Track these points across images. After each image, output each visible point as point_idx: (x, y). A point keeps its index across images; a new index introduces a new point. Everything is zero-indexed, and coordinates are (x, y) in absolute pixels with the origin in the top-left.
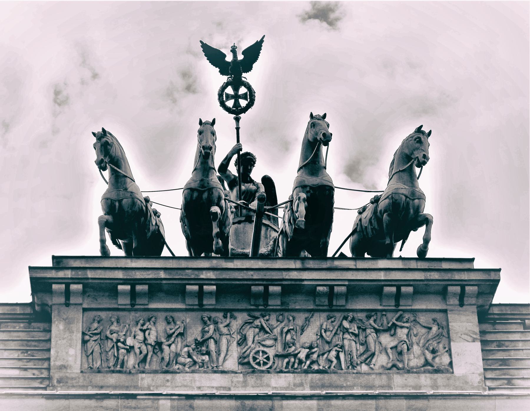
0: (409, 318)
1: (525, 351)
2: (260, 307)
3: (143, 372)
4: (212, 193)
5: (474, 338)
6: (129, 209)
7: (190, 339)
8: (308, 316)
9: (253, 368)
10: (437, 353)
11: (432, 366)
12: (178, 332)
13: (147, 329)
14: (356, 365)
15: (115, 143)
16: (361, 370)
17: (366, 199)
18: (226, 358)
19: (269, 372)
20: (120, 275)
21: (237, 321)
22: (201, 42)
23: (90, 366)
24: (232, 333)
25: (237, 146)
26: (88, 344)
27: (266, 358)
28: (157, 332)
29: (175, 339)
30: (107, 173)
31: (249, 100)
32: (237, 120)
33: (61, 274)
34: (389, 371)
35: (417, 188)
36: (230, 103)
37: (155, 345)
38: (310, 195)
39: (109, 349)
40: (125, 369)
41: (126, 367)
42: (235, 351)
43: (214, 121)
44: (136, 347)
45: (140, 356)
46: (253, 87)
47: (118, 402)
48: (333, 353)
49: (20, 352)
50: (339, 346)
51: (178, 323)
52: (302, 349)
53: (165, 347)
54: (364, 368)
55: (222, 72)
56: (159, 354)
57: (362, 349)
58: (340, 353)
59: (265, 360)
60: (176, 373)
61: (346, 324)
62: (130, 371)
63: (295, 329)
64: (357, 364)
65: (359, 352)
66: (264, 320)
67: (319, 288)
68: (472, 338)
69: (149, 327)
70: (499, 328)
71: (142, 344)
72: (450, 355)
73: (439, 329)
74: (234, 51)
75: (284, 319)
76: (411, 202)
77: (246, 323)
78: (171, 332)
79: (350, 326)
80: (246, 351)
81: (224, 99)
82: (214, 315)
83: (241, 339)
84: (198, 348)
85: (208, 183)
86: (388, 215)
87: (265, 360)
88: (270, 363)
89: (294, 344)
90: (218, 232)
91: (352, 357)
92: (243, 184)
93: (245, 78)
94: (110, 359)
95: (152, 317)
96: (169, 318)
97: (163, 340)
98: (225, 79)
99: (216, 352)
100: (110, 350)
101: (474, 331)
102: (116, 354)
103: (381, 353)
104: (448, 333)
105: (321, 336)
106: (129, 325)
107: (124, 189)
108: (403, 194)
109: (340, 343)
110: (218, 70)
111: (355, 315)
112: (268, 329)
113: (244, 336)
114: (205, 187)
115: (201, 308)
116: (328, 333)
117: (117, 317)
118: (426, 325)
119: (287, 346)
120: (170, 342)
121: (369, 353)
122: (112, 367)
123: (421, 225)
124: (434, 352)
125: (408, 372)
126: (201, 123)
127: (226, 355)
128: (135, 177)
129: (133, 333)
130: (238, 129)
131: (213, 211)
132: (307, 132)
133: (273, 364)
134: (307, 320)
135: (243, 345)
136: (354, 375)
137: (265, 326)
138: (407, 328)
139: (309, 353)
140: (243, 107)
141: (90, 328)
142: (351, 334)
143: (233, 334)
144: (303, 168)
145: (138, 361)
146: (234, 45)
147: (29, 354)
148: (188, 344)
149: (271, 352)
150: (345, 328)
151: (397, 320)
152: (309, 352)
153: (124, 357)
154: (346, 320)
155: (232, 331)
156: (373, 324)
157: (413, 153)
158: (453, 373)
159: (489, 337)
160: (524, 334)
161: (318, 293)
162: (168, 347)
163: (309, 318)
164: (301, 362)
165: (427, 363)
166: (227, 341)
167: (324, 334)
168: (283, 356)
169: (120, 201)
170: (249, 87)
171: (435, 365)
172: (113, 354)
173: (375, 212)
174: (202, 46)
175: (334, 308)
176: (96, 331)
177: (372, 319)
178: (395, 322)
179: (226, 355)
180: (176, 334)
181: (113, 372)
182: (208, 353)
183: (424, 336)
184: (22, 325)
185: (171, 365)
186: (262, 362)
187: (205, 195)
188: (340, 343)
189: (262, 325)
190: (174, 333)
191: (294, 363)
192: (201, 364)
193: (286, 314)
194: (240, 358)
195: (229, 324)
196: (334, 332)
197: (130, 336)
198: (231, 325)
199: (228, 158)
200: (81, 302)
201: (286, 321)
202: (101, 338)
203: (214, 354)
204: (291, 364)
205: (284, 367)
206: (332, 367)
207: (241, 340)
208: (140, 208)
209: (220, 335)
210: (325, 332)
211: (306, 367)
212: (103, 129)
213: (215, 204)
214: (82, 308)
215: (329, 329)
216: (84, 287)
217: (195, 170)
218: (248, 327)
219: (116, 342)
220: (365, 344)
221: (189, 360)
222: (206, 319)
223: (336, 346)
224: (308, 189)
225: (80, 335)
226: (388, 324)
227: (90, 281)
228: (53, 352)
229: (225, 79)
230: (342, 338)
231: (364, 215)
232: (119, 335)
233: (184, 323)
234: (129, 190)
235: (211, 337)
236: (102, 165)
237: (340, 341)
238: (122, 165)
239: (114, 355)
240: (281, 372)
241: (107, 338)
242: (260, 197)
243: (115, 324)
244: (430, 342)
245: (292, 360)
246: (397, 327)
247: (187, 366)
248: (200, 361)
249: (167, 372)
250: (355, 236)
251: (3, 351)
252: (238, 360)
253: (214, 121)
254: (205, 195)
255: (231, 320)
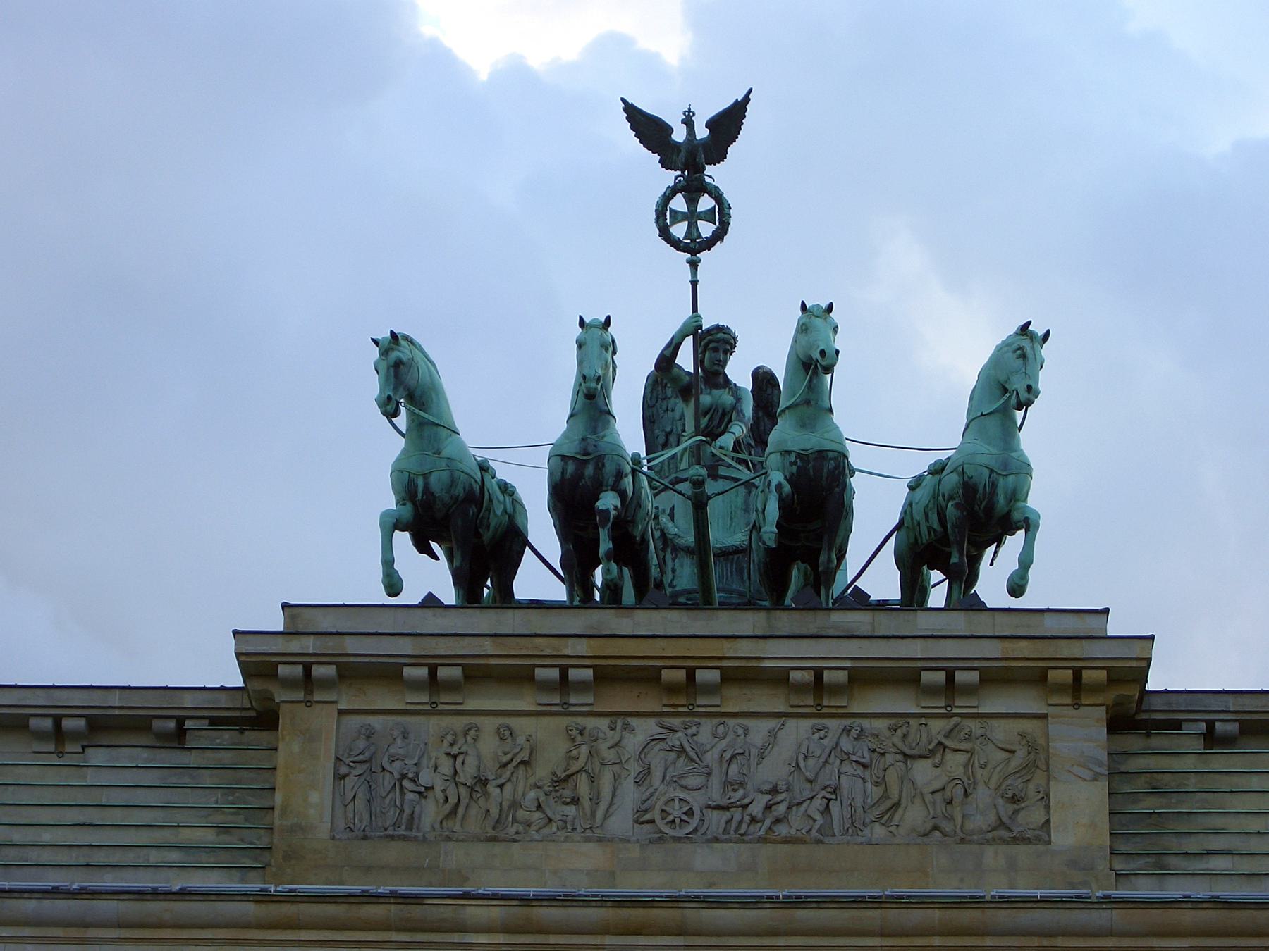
0: (971, 731)
1: (1198, 796)
2: (681, 709)
3: (449, 839)
4: (603, 465)
5: (1097, 773)
6: (444, 491)
7: (542, 772)
8: (774, 726)
9: (661, 832)
10: (1024, 802)
11: (1012, 831)
12: (519, 760)
13: (459, 753)
14: (861, 827)
15: (418, 356)
16: (872, 835)
17: (921, 463)
18: (611, 810)
19: (691, 841)
20: (406, 647)
21: (635, 736)
22: (623, 100)
23: (348, 826)
24: (623, 761)
25: (692, 321)
26: (347, 779)
27: (685, 813)
28: (479, 757)
29: (512, 773)
30: (402, 421)
31: (717, 223)
32: (694, 264)
33: (295, 646)
34: (925, 839)
35: (1016, 451)
36: (679, 230)
37: (475, 784)
38: (797, 471)
39: (386, 794)
40: (414, 833)
41: (417, 828)
42: (630, 795)
43: (608, 319)
44: (438, 788)
45: (445, 807)
46: (728, 196)
47: (390, 911)
48: (818, 803)
49: (220, 792)
50: (829, 790)
51: (521, 740)
52: (756, 794)
53: (493, 790)
54: (879, 831)
55: (666, 164)
56: (481, 801)
57: (876, 792)
58: (831, 802)
59: (685, 817)
60: (515, 841)
61: (846, 744)
62: (424, 836)
63: (747, 754)
64: (864, 824)
65: (869, 800)
66: (687, 735)
67: (795, 676)
68: (1092, 773)
69: (462, 750)
70: (1157, 742)
71: (448, 783)
72: (1047, 807)
73: (1029, 753)
74: (688, 121)
75: (728, 731)
76: (1001, 480)
77: (653, 740)
78: (505, 759)
79: (854, 748)
80: (648, 800)
81: (668, 221)
82: (590, 723)
83: (639, 774)
84: (557, 791)
85: (595, 446)
86: (957, 506)
87: (685, 817)
88: (694, 822)
89: (741, 784)
90: (610, 549)
91: (855, 811)
92: (709, 390)
93: (711, 177)
94: (388, 812)
95: (469, 729)
96: (504, 730)
97: (491, 777)
98: (669, 177)
99: (591, 799)
100: (387, 795)
101: (1098, 759)
102: (398, 803)
103: (913, 803)
104: (1048, 765)
105: (798, 765)
106: (426, 744)
107: (433, 451)
108: (984, 466)
109: (831, 783)
110: (656, 157)
111: (866, 723)
112: (692, 754)
113: (647, 767)
114: (590, 454)
115: (566, 710)
116: (811, 762)
117: (402, 729)
118: (1003, 746)
119: (729, 786)
120: (502, 780)
121: (888, 804)
122: (391, 828)
123: (1019, 529)
124: (1015, 799)
125: (962, 841)
126: (582, 323)
127: (611, 804)
128: (459, 426)
129: (434, 758)
130: (694, 284)
131: (600, 508)
132: (795, 341)
133: (701, 823)
134: (773, 734)
135: (644, 785)
136: (856, 847)
137: (688, 749)
138: (967, 752)
139: (771, 802)
140: (706, 238)
141: (351, 750)
142: (854, 764)
143: (625, 762)
144: (787, 411)
145: (439, 819)
146: (689, 109)
147: (238, 797)
148: (538, 784)
149: (696, 800)
150: (845, 752)
151: (947, 736)
152: (770, 800)
153: (414, 807)
154: (848, 735)
155: (624, 755)
156: (900, 745)
157: (1009, 379)
158: (1049, 843)
159: (1134, 765)
160: (1204, 756)
161: (792, 684)
162: (498, 790)
163: (776, 731)
164: (753, 820)
165: (1001, 824)
166: (615, 776)
167: (802, 764)
168: (726, 808)
169: (426, 476)
170: (718, 196)
171: (1017, 829)
172: (393, 803)
173: (935, 496)
174: (625, 110)
175: (825, 710)
176: (361, 758)
177: (899, 732)
178: (944, 741)
179: (611, 804)
180: (514, 764)
181: (392, 837)
182: (575, 801)
183: (998, 768)
184: (227, 735)
185: (504, 824)
186: (677, 821)
187: (589, 470)
188: (833, 782)
189: (681, 745)
190: (512, 760)
191: (741, 822)
192: (560, 823)
193: (731, 722)
194: (638, 811)
195: (620, 741)
196: (822, 759)
197: (428, 767)
198: (623, 743)
199: (674, 342)
200: (334, 698)
201: (731, 736)
202: (371, 770)
203: (586, 802)
204: (734, 825)
205: (721, 830)
206: (814, 832)
207: (641, 776)
208: (467, 489)
209: (602, 764)
210: (806, 758)
211: (762, 832)
212: (392, 332)
213: (609, 488)
214: (336, 711)
215: (813, 753)
216: (338, 670)
217: (572, 416)
218: (659, 746)
219: (398, 780)
220: (880, 782)
221: (538, 815)
222: (575, 732)
223: (823, 789)
224: (793, 458)
225: (330, 765)
226: (930, 744)
227: (352, 659)
228: (279, 798)
229: (669, 177)
230: (838, 771)
231: (919, 493)
232: (406, 764)
233: (531, 741)
234: (445, 453)
235: (581, 770)
236: (389, 407)
237: (833, 778)
238: (432, 400)
239: (396, 806)
240: (717, 840)
241: (384, 769)
242: (694, 478)
243: (399, 741)
244: (1008, 782)
245: (737, 814)
246: (947, 750)
247: (533, 828)
248: (559, 817)
249: (494, 839)
250: (903, 531)
251: (189, 791)
252: (634, 815)
253: (608, 319)
254: (589, 470)
255: (624, 733)
